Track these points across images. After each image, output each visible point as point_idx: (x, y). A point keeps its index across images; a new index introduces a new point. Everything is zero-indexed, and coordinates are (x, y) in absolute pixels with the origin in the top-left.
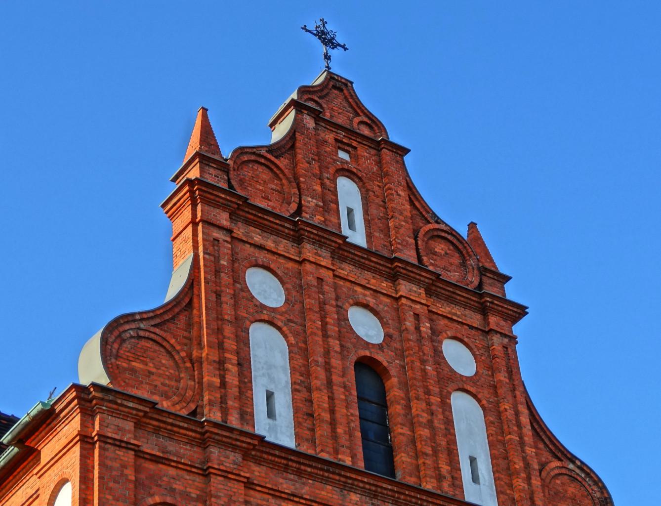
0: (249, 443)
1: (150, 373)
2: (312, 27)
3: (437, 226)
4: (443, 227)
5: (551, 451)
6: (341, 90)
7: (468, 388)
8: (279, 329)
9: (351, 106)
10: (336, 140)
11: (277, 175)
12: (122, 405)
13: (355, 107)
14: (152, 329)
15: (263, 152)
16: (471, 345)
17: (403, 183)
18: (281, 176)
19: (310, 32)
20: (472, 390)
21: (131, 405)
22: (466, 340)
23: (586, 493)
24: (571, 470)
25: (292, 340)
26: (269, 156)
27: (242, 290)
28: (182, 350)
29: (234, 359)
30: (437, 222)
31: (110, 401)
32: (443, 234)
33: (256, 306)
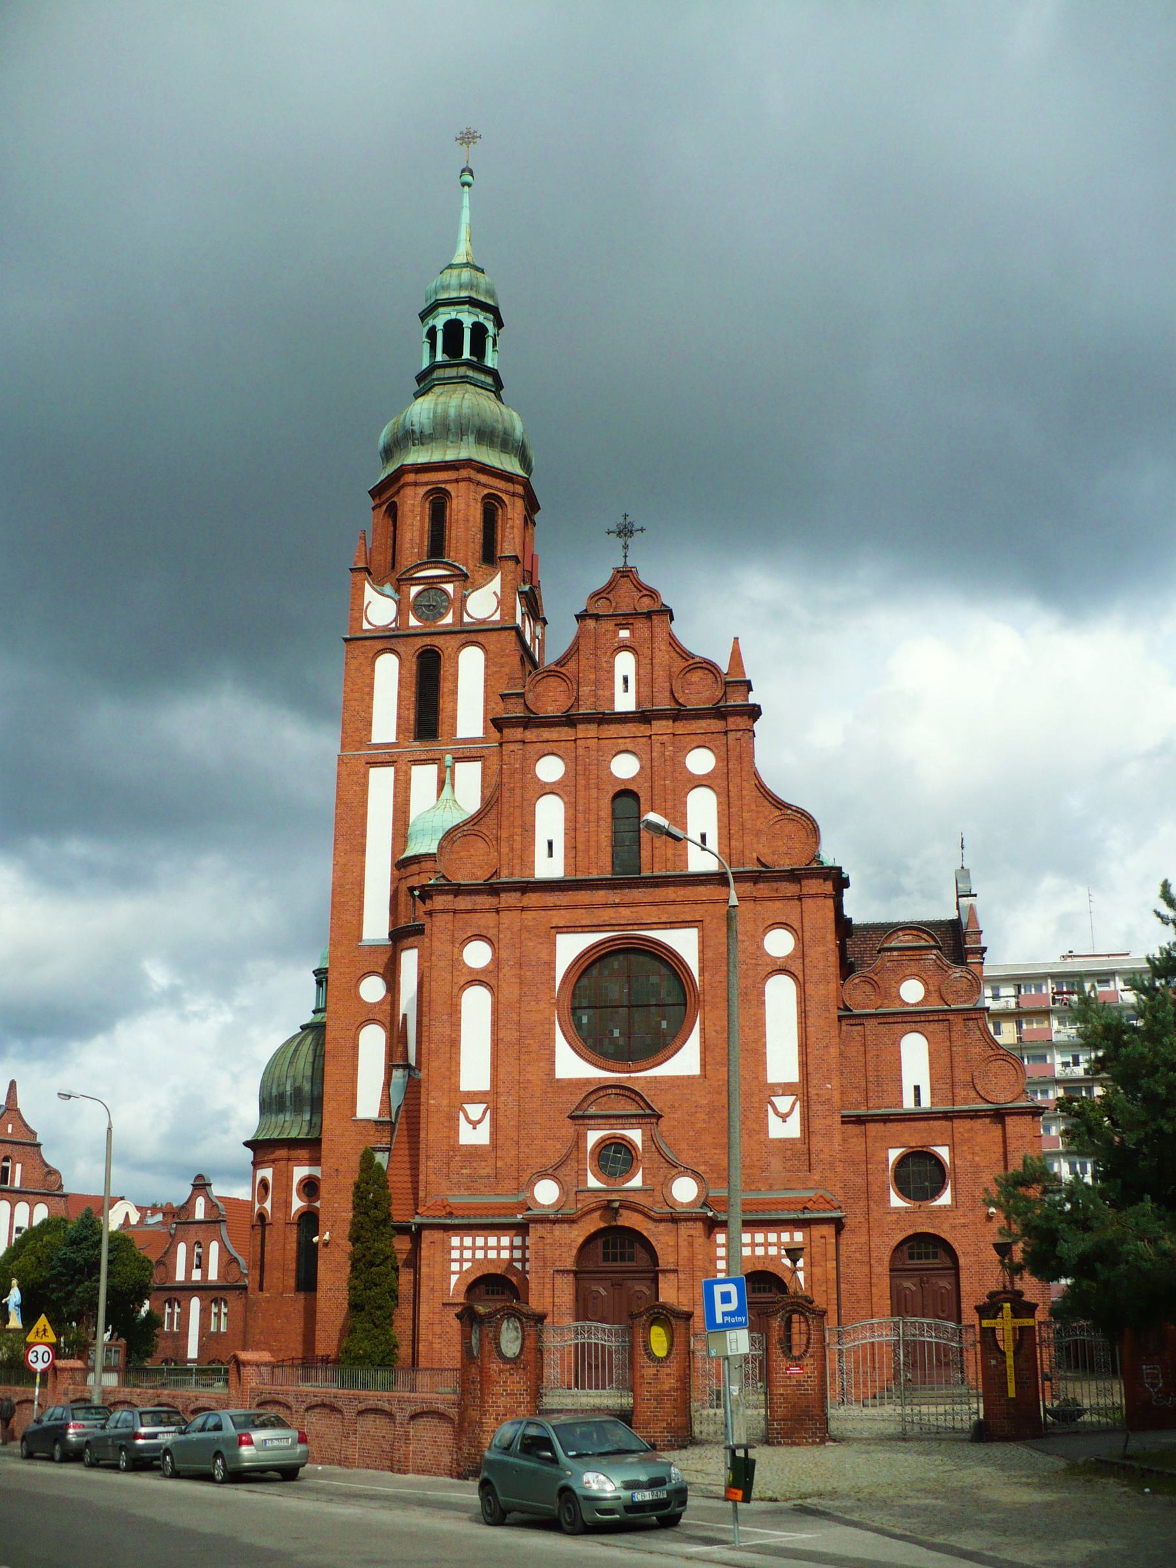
3: (691, 662)
4: (697, 660)
9: (635, 586)
30: (693, 658)
32: (699, 665)
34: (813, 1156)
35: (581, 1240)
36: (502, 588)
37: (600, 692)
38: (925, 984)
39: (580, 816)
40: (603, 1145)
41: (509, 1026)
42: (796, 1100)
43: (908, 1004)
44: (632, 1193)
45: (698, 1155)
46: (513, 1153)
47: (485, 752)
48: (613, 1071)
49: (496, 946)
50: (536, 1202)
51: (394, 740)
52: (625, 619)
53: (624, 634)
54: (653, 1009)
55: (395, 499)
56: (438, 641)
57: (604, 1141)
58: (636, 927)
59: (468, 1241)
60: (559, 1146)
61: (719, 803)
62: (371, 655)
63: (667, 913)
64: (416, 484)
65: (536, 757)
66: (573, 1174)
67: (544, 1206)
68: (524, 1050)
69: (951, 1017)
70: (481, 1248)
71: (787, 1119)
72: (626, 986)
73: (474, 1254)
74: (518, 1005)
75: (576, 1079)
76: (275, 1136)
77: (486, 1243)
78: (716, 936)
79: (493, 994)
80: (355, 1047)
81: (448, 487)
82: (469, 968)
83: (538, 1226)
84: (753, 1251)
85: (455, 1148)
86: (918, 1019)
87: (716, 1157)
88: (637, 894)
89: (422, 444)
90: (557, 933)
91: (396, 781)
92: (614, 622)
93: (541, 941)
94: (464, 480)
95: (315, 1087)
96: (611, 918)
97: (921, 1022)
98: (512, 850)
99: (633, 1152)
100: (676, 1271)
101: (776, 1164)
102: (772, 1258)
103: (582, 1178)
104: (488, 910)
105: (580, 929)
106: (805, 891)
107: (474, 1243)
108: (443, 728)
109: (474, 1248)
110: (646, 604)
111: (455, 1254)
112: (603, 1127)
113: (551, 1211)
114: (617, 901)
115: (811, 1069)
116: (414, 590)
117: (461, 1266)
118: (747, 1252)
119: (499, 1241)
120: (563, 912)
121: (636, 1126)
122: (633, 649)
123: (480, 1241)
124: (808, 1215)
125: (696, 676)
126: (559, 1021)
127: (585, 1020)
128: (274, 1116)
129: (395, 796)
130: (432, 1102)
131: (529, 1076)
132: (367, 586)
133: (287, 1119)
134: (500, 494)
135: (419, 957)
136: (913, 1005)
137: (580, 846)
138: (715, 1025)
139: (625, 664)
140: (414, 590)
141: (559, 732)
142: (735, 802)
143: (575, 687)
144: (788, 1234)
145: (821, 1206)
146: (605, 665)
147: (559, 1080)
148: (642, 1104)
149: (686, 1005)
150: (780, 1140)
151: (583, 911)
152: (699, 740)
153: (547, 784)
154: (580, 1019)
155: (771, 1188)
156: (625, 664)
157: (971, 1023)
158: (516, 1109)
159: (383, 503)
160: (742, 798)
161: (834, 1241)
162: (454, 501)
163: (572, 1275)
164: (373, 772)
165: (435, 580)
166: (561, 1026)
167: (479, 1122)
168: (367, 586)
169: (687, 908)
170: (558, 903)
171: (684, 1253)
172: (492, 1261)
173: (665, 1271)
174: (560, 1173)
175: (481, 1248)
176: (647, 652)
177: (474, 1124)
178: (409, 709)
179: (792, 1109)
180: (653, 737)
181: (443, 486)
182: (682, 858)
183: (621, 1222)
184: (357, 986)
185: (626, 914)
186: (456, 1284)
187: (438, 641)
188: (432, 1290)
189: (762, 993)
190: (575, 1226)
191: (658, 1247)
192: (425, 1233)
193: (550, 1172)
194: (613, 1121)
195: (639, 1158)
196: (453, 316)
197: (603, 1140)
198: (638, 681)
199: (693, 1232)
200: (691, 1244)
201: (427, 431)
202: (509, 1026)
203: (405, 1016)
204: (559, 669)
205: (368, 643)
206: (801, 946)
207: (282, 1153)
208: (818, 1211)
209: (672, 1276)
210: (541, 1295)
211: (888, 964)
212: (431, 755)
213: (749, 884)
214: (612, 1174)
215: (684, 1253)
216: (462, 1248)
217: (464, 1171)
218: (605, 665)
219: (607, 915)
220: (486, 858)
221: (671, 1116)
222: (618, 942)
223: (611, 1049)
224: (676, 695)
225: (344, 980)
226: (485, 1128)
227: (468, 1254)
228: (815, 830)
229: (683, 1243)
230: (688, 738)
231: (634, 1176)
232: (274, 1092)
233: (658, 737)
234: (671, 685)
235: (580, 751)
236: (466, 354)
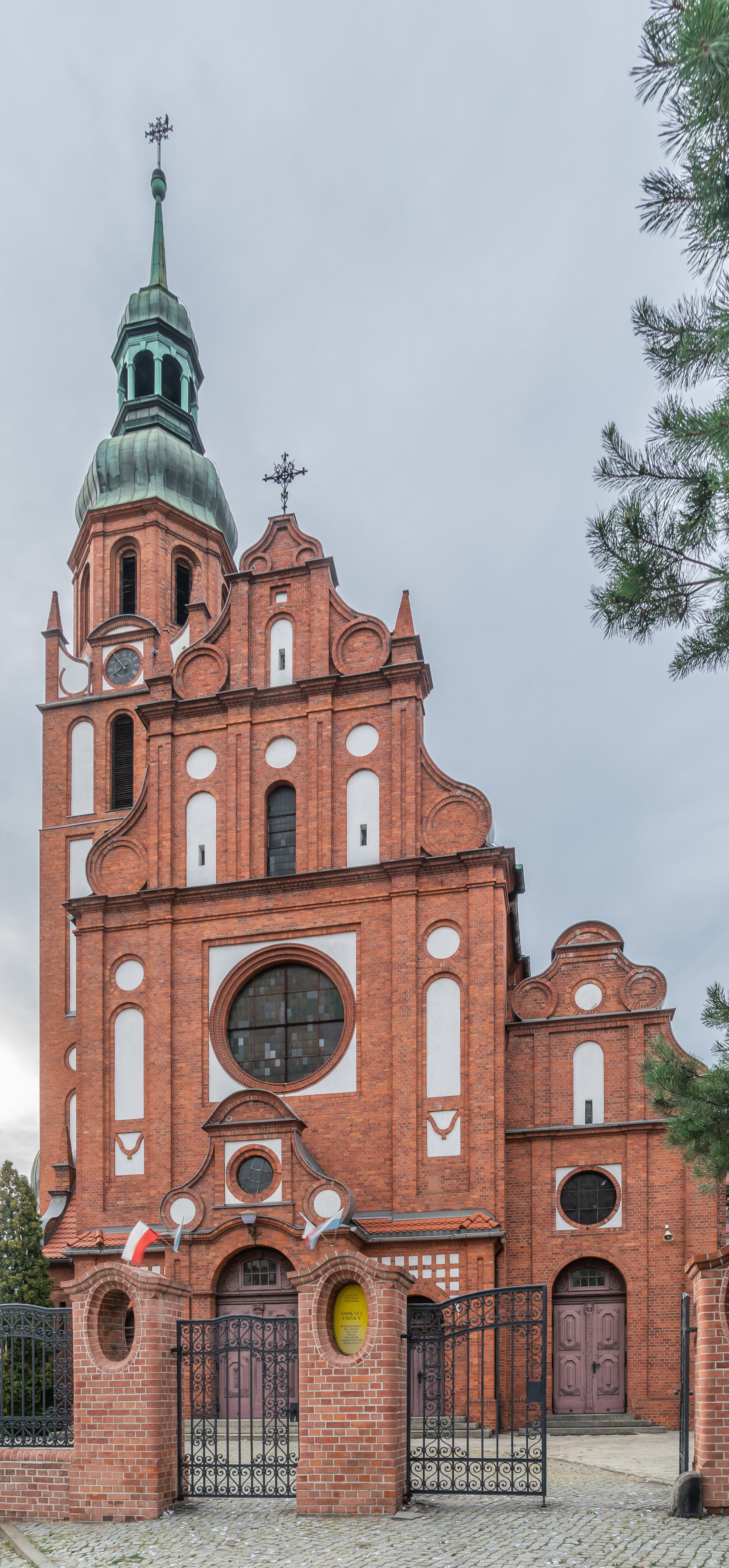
1: (122, 870)
34: (473, 1174)
38: (603, 987)
40: (241, 1159)
42: (457, 1115)
43: (582, 1011)
44: (270, 1209)
45: (353, 1176)
57: (242, 1154)
58: (290, 935)
66: (210, 1191)
69: (630, 1023)
78: (375, 939)
79: (145, 1018)
86: (593, 1026)
87: (371, 1178)
97: (596, 1029)
99: (273, 1165)
102: (426, 1282)
105: (232, 942)
115: (473, 1079)
120: (215, 923)
124: (463, 1235)
136: (588, 1012)
138: (372, 1037)
144: (443, 1256)
145: (479, 1225)
151: (235, 920)
155: (427, 1210)
157: (652, 1030)
161: (492, 1262)
170: (209, 913)
183: (263, 1241)
193: (185, 1190)
195: (279, 1171)
197: (242, 1153)
208: (476, 1230)
211: (563, 968)
214: (252, 1191)
220: (136, 870)
221: (327, 1136)
222: (273, 954)
231: (273, 1190)
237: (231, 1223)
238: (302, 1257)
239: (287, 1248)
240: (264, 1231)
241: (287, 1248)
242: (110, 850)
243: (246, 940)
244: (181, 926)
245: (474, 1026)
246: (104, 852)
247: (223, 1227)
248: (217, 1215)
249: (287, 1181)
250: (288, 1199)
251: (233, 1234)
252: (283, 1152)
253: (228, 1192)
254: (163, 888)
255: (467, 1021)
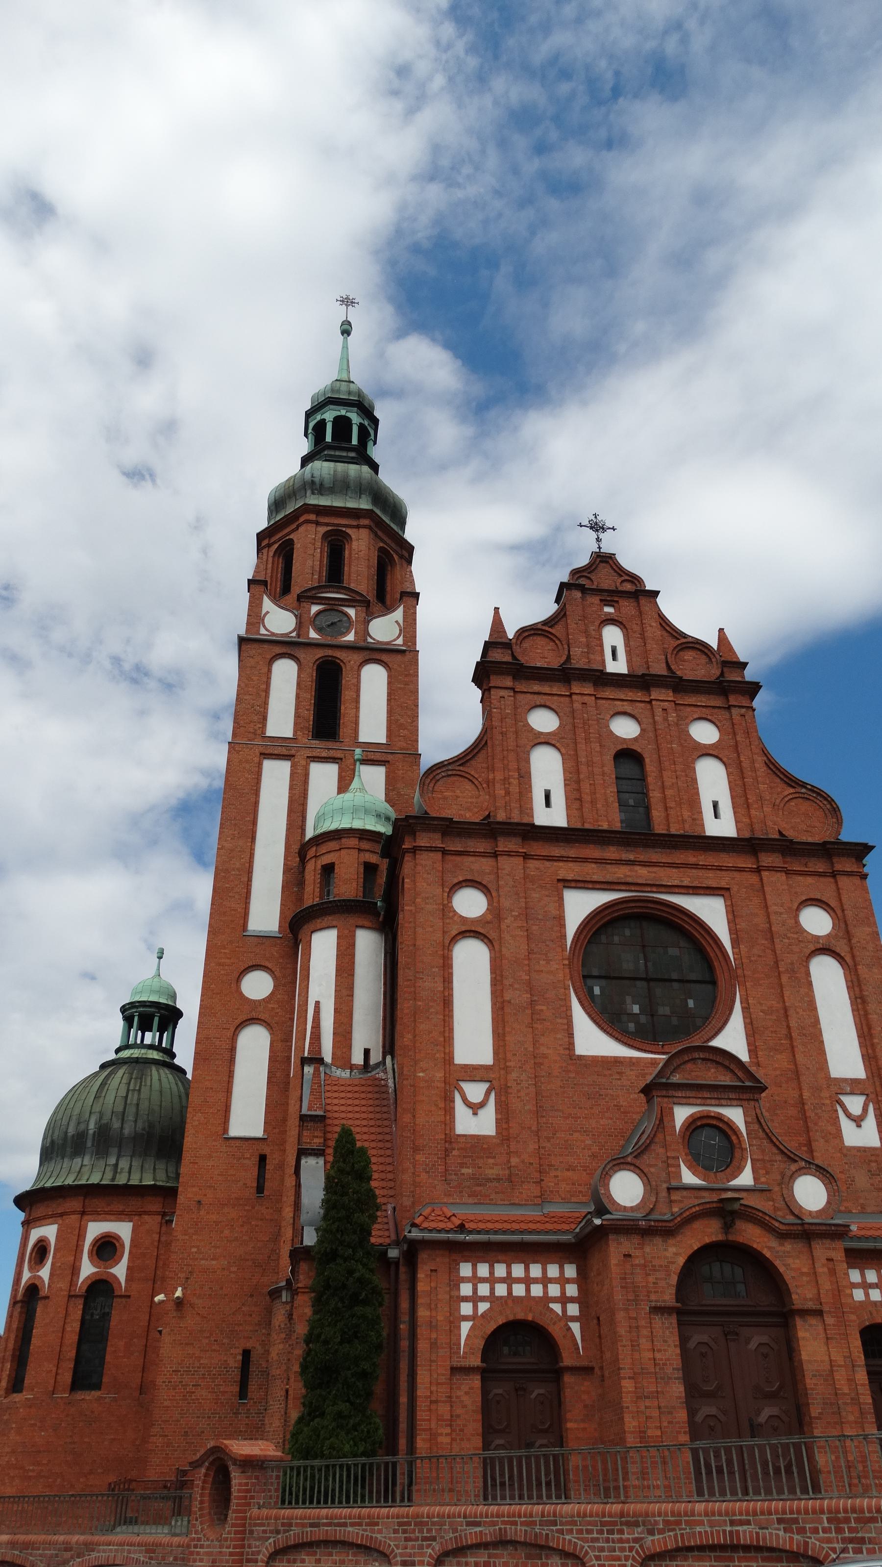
0: (524, 830)
1: (458, 797)
2: (586, 523)
3: (684, 640)
4: (690, 640)
5: (786, 783)
6: (607, 562)
7: (711, 752)
8: (554, 746)
10: (601, 600)
11: (551, 639)
12: (431, 824)
13: (618, 571)
14: (458, 768)
15: (540, 626)
16: (713, 720)
17: (656, 616)
18: (554, 639)
19: (584, 526)
20: (714, 753)
21: (436, 823)
22: (709, 717)
23: (818, 807)
24: (804, 793)
25: (563, 750)
26: (544, 628)
27: (524, 726)
28: (480, 776)
29: (516, 775)
30: (685, 638)
31: (422, 824)
32: (691, 645)
33: (535, 734)
35: (681, 1261)
36: (404, 618)
37: (592, 656)
39: (583, 768)
40: (693, 1127)
41: (516, 986)
46: (532, 1146)
47: (390, 758)
48: (645, 1051)
49: (494, 894)
50: (614, 1202)
51: (291, 736)
52: (611, 596)
53: (608, 610)
54: (676, 985)
55: (291, 537)
56: (338, 654)
58: (654, 890)
59: (483, 1270)
60: (588, 1142)
61: (729, 774)
62: (269, 657)
63: (689, 876)
64: (318, 523)
65: (527, 707)
66: (660, 1164)
67: (625, 1208)
68: (536, 1017)
70: (502, 1280)
71: (863, 1124)
72: (641, 955)
73: (492, 1290)
74: (526, 962)
75: (602, 1057)
76: (69, 1181)
77: (509, 1273)
80: (233, 1050)
81: (349, 531)
82: (461, 916)
83: (623, 1239)
84: (867, 1295)
85: (450, 1139)
88: (655, 855)
89: (322, 495)
90: (565, 887)
91: (292, 774)
92: (598, 598)
93: (547, 893)
94: (365, 527)
95: (125, 1126)
96: (626, 876)
98: (508, 793)
99: (734, 1138)
100: (819, 1313)
101: (862, 1180)
103: (672, 1169)
104: (483, 855)
105: (590, 886)
106: (838, 867)
107: (492, 1272)
108: (344, 731)
109: (492, 1280)
110: (628, 587)
111: (466, 1289)
112: (691, 1101)
113: (639, 1215)
114: (632, 857)
116: (315, 609)
117: (475, 1308)
118: (858, 1295)
119: (527, 1269)
120: (571, 864)
121: (735, 1103)
122: (621, 623)
123: (500, 1270)
125: (689, 655)
126: (574, 987)
127: (597, 991)
128: (66, 1160)
129: (291, 788)
130: (421, 1074)
131: (544, 1050)
132: (265, 597)
133: (85, 1163)
134: (392, 553)
135: (338, 937)
137: (587, 798)
138: (761, 1004)
139: (612, 636)
140: (315, 609)
141: (551, 686)
142: (748, 773)
143: (566, 646)
146: (593, 633)
147: (581, 1057)
148: (740, 1074)
149: (714, 983)
150: (859, 1149)
151: (593, 865)
152: (698, 712)
153: (542, 733)
154: (591, 990)
155: (863, 1211)
156: (612, 636)
158: (532, 1089)
159: (275, 543)
160: (754, 770)
162: (355, 545)
163: (675, 1316)
164: (269, 766)
165: (337, 603)
166: (576, 993)
167: (482, 1104)
168: (265, 597)
169: (711, 874)
170: (565, 854)
171: (826, 1285)
172: (519, 1299)
173: (805, 1313)
174: (647, 1159)
175: (502, 1280)
176: (637, 628)
177: (475, 1108)
178: (307, 710)
179: (865, 1110)
180: (654, 703)
181: (344, 529)
182: (698, 822)
184: (239, 980)
185: (643, 874)
186: (468, 1335)
187: (338, 654)
188: (434, 1345)
189: (808, 974)
190: (671, 1241)
191: (788, 1275)
192: (423, 1256)
193: (629, 1159)
194: (707, 1095)
196: (343, 412)
198: (629, 653)
199: (832, 1254)
200: (833, 1272)
201: (327, 484)
202: (516, 986)
203: (317, 1004)
204: (547, 629)
205: (266, 646)
206: (843, 926)
207: (75, 1204)
209: (813, 1321)
210: (635, 1346)
212: (332, 753)
213: (777, 855)
215: (826, 1285)
216: (475, 1280)
217: (464, 1171)
218: (593, 633)
219: (621, 873)
220: (474, 800)
223: (632, 1026)
224: (673, 667)
225: (222, 972)
226: (489, 1113)
227: (484, 1289)
228: (835, 811)
229: (822, 1270)
230: (689, 709)
231: (740, 1170)
232: (71, 1131)
233: (658, 703)
234: (666, 658)
235: (577, 706)
236: (355, 441)
237: (697, 1209)
238: (790, 1261)
239: (769, 1248)
240: (740, 1225)
241: (769, 1248)
242: (443, 777)
243: (602, 886)
244: (531, 861)
245: (871, 1007)
246: (438, 777)
247: (688, 1213)
248: (675, 1196)
249: (758, 1160)
250: (762, 1183)
251: (697, 1225)
252: (746, 1122)
253: (684, 1169)
254: (512, 821)
255: (859, 1001)
